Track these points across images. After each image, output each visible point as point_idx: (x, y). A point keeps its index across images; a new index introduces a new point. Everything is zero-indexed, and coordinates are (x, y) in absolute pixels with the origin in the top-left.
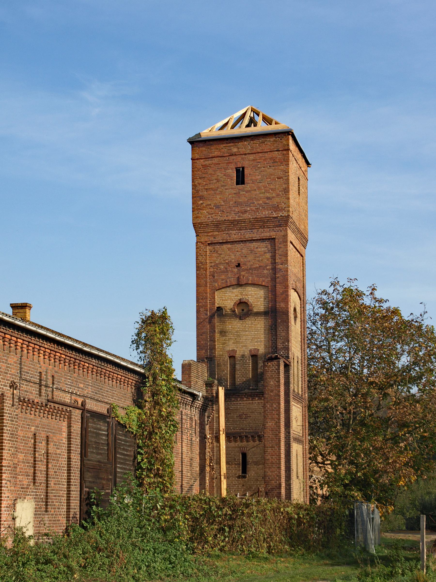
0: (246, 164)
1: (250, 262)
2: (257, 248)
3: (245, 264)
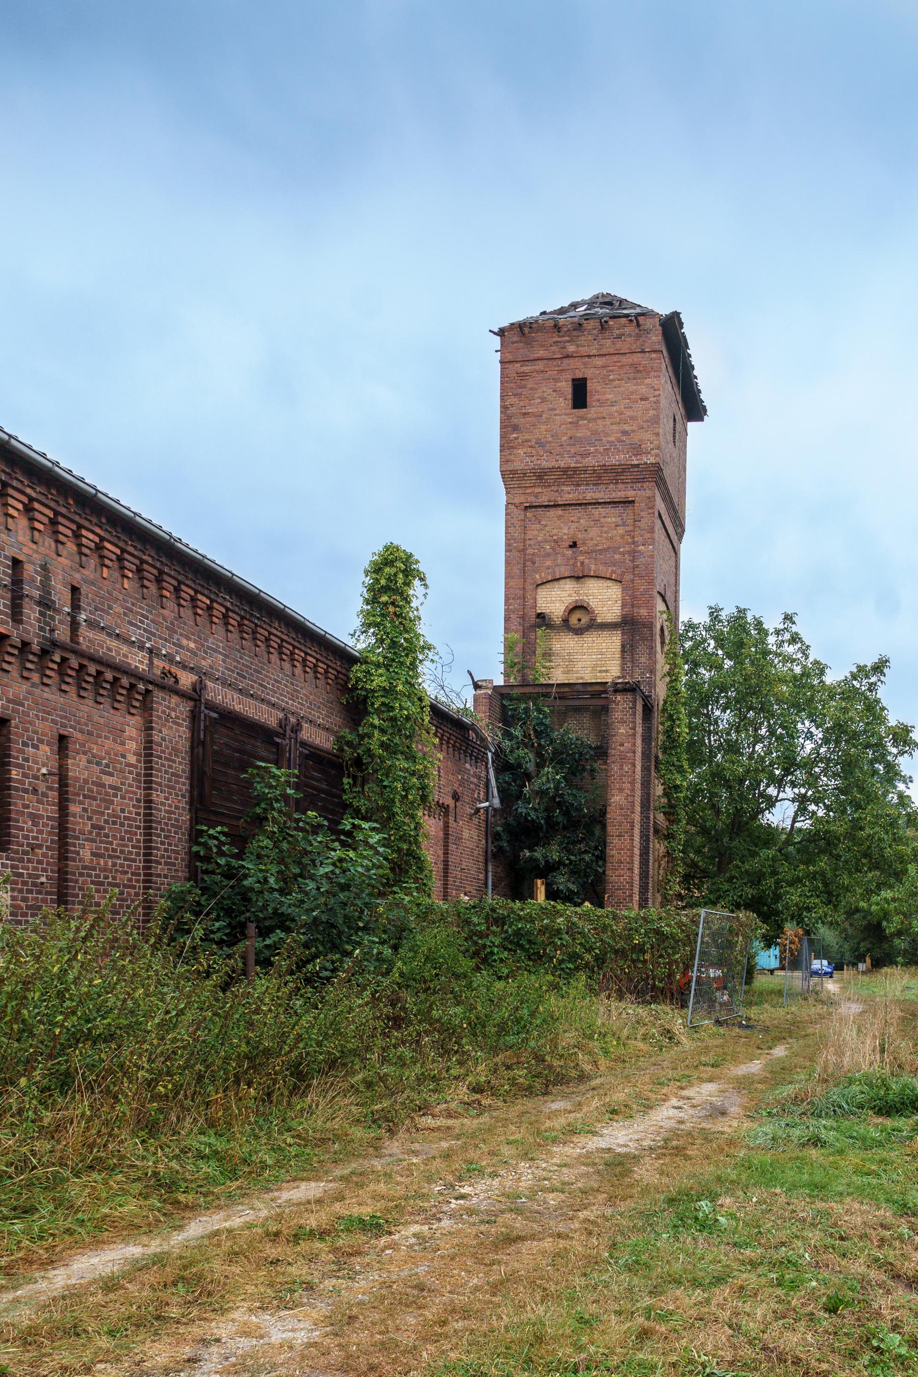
0: (588, 373)
1: (592, 539)
2: (605, 517)
3: (584, 543)
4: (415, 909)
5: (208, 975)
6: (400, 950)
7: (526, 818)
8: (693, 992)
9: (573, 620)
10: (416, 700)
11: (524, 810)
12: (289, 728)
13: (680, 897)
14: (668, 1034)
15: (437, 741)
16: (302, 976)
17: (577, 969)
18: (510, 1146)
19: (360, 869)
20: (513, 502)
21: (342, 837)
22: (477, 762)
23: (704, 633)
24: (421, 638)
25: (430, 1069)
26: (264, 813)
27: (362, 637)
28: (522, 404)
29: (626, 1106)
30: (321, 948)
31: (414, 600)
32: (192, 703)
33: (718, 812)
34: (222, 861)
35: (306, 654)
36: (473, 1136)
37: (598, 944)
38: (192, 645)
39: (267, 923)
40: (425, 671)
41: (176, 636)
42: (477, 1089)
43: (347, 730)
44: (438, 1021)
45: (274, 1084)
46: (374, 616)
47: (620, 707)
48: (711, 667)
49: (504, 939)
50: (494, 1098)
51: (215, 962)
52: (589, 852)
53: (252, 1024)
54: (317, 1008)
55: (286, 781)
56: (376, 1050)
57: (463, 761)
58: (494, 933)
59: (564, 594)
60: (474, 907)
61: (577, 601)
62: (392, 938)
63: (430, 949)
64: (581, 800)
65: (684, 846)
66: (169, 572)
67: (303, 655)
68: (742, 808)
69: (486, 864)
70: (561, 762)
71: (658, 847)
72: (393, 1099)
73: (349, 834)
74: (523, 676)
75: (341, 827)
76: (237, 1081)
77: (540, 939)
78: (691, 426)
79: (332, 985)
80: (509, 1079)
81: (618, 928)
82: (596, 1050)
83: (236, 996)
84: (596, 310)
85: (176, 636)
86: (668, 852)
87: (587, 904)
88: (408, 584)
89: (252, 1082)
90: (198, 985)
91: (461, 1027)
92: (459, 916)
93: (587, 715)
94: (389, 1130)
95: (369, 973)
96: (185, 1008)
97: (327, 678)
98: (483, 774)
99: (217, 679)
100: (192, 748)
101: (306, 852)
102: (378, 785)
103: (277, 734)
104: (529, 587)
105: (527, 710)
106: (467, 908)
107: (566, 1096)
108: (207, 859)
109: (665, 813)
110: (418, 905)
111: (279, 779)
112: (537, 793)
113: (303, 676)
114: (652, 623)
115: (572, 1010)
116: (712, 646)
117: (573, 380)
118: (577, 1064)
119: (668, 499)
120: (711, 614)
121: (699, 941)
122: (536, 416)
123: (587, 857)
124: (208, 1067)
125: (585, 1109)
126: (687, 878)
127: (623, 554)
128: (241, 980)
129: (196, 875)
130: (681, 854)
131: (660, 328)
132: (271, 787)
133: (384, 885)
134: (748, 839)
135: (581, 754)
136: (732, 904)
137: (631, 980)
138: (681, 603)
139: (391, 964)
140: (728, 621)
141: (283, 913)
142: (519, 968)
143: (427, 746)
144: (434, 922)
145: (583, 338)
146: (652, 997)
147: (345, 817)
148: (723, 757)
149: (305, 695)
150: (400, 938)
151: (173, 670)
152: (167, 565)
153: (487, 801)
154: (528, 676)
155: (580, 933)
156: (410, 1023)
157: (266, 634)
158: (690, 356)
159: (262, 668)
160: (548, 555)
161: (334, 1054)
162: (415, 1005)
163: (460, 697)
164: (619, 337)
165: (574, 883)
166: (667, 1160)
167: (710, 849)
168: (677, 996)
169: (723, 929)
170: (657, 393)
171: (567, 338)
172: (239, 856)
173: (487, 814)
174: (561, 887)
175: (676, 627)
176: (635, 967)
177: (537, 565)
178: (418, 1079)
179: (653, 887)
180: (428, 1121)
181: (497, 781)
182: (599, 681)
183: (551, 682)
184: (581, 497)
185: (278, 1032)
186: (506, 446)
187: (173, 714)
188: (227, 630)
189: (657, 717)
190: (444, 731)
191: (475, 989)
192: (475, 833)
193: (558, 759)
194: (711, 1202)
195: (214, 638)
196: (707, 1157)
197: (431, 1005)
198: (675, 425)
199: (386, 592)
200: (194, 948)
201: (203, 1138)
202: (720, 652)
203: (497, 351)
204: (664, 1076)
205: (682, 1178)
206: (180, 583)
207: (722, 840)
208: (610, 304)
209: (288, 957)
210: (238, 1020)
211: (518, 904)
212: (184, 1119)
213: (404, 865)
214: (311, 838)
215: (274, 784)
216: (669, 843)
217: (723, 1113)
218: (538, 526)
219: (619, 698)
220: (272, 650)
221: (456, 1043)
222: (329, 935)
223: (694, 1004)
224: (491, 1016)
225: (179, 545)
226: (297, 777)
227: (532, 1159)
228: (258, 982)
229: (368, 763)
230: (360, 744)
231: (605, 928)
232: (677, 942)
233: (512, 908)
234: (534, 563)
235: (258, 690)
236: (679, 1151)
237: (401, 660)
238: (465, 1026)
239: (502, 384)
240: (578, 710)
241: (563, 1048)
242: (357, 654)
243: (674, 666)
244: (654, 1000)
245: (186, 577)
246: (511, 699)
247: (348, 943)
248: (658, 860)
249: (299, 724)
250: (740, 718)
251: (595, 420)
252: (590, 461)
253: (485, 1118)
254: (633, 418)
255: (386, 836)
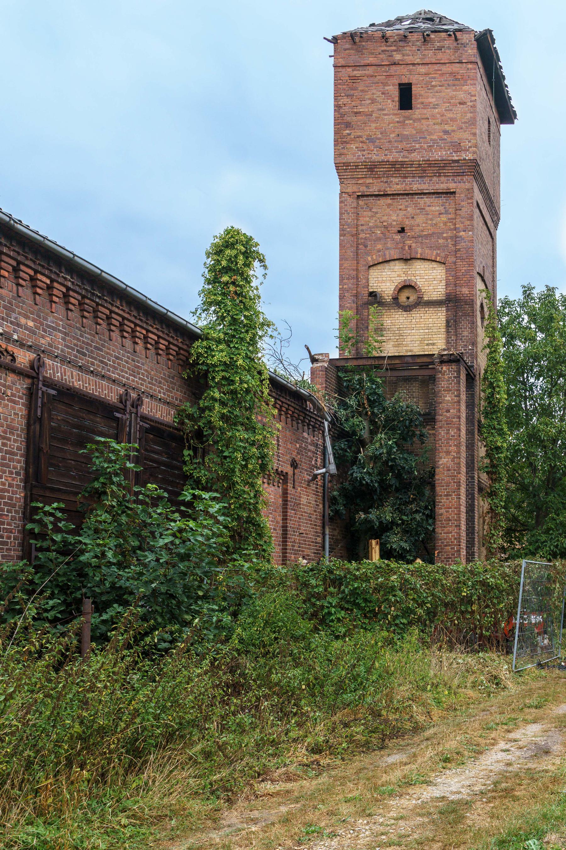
0: (413, 79)
1: (418, 225)
2: (429, 206)
3: (411, 229)
4: (254, 575)
5: (40, 655)
6: (240, 617)
7: (361, 482)
8: (516, 638)
9: (402, 298)
10: (255, 373)
11: (359, 475)
12: (130, 402)
13: (503, 549)
14: (495, 680)
15: (276, 412)
16: (140, 649)
17: (410, 623)
18: (348, 804)
19: (200, 539)
20: (347, 191)
21: (182, 508)
22: (314, 431)
23: (518, 309)
24: (261, 316)
25: (270, 734)
26: (103, 487)
27: (204, 315)
28: (353, 104)
29: (458, 753)
30: (160, 620)
31: (254, 280)
32: (29, 381)
33: (534, 470)
34: (58, 538)
35: (148, 331)
36: (312, 797)
37: (429, 599)
38: (31, 324)
39: (104, 598)
40: (265, 346)
41: (14, 315)
42: (316, 750)
43: (188, 404)
44: (277, 684)
45: (109, 764)
46: (215, 295)
47: (446, 377)
48: (525, 339)
49: (341, 599)
50: (332, 757)
51: (48, 642)
52: (420, 512)
53: (86, 703)
54: (154, 681)
55: (126, 455)
56: (215, 718)
57: (301, 431)
58: (331, 594)
59: (394, 274)
60: (312, 570)
61: (405, 281)
62: (232, 605)
63: (270, 614)
64: (412, 464)
65: (505, 502)
66: (8, 252)
67: (144, 332)
68: (555, 465)
69: (324, 527)
70: (393, 429)
71: (483, 504)
72: (232, 768)
73: (189, 504)
74: (357, 350)
75: (181, 498)
76: (69, 764)
77: (375, 597)
78: (504, 128)
79: (171, 656)
80: (347, 737)
81: (447, 582)
82: (429, 701)
83: (70, 675)
84: (419, 24)
85: (14, 315)
86: (491, 509)
87: (419, 561)
88: (248, 265)
89: (85, 764)
90: (28, 666)
91: (300, 689)
92: (297, 579)
93: (416, 384)
94: (229, 800)
95: (208, 641)
96: (14, 692)
97: (168, 354)
98: (320, 442)
99: (57, 357)
100: (28, 425)
101: (145, 525)
102: (218, 456)
103: (118, 410)
104: (362, 268)
105: (360, 381)
106: (305, 572)
107: (401, 749)
108: (42, 536)
109: (488, 473)
110: (258, 571)
111: (118, 453)
112: (371, 458)
113: (144, 352)
114: (472, 301)
115: (406, 664)
116: (525, 321)
117: (400, 85)
118: (412, 716)
119: (484, 190)
120: (525, 292)
121: (521, 590)
122: (367, 115)
123: (418, 517)
124: (38, 752)
125: (420, 760)
126: (509, 532)
127: (446, 239)
128: (76, 659)
129: (30, 554)
130: (503, 510)
131: (475, 43)
132: (110, 461)
133: (223, 553)
134: (561, 494)
135: (411, 421)
136: (550, 554)
137: (460, 631)
138: (498, 282)
139: (231, 630)
140: (539, 299)
141: (120, 587)
142: (355, 627)
143: (266, 417)
144: (273, 587)
145: (408, 48)
146: (479, 645)
147: (185, 488)
148: (538, 420)
149: (146, 371)
150: (240, 605)
151: (10, 349)
152: (6, 246)
153: (324, 467)
154: (361, 350)
155: (412, 589)
156: (250, 688)
157: (108, 312)
158: (501, 67)
159: (103, 346)
160: (379, 239)
161: (172, 726)
162: (254, 670)
163: (298, 371)
164: (440, 49)
165: (406, 541)
166: (497, 803)
167: (529, 504)
168: (502, 643)
169: (542, 578)
170: (473, 98)
171: (394, 48)
172: (76, 532)
173: (324, 480)
174: (394, 546)
175: (494, 304)
176: (464, 618)
177: (369, 248)
178: (257, 745)
179: (479, 541)
180: (268, 787)
181: (333, 447)
182: (427, 353)
183: (383, 355)
184: (408, 188)
185: (114, 709)
186: (340, 141)
187: (9, 392)
188: (68, 309)
189: (479, 386)
190: (282, 402)
191: (314, 650)
192: (312, 498)
193: (390, 425)
194: (538, 840)
195: (54, 317)
196: (534, 796)
197: (270, 669)
198: (489, 126)
199: (226, 273)
200: (26, 628)
201: (30, 829)
202: (533, 326)
203: (330, 56)
204: (493, 721)
205: (512, 818)
206: (19, 263)
207: (539, 495)
208: (431, 20)
209: (125, 631)
210: (71, 700)
211: (354, 564)
212: (10, 810)
213: (244, 532)
214: (150, 510)
215: (113, 458)
216: (492, 500)
217: (547, 752)
218: (370, 214)
219: (444, 368)
220: (113, 328)
221: (295, 705)
222: (168, 606)
223: (519, 649)
224: (329, 676)
225: (19, 226)
226: (137, 450)
227: (370, 815)
228: (93, 658)
229: (208, 434)
230: (201, 417)
231: (436, 582)
232: (501, 592)
233: (348, 569)
234: (366, 247)
235: (99, 366)
236: (508, 793)
237: (242, 336)
238: (304, 687)
239: (335, 85)
240: (407, 380)
241: (398, 702)
242: (199, 331)
243: (493, 338)
244: (482, 648)
245: (26, 257)
246: (346, 371)
247: (187, 613)
248: (482, 517)
249: (139, 399)
250: (551, 384)
251: (419, 120)
252: (415, 156)
253: (324, 779)
254: (452, 119)
255: (226, 505)
